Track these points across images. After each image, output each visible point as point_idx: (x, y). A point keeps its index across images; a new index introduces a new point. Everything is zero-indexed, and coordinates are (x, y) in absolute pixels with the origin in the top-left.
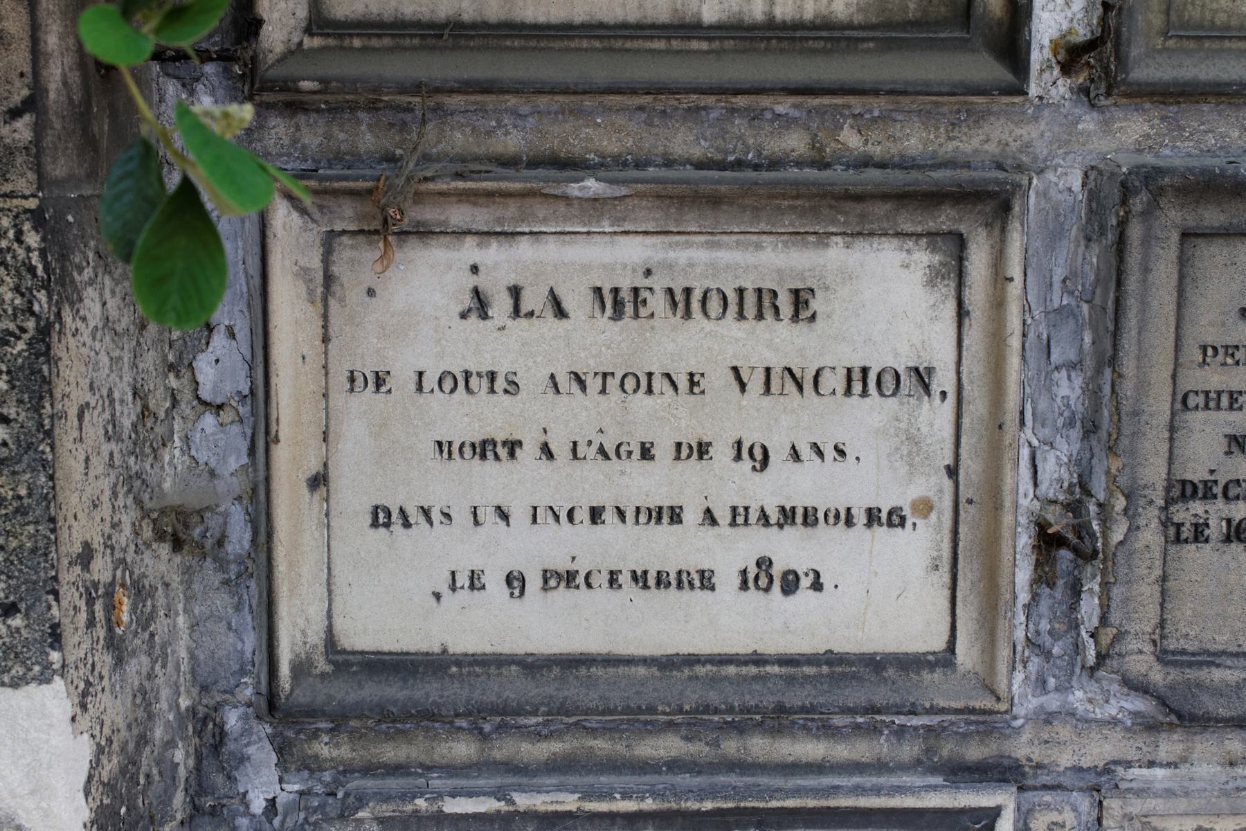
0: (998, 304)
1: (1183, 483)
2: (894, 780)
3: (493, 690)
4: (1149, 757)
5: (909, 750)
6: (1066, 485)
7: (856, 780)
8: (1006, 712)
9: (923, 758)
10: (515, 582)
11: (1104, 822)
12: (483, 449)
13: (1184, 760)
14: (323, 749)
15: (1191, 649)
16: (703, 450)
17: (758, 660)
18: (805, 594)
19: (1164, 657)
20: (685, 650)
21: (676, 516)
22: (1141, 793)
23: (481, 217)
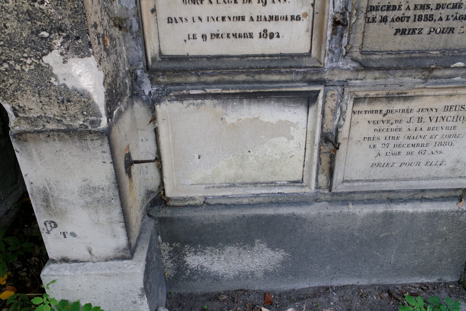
1: (371, 6)
2: (296, 85)
3: (201, 64)
4: (356, 78)
5: (299, 77)
6: (341, 8)
7: (287, 85)
8: (323, 67)
9: (303, 79)
10: (204, 37)
11: (344, 93)
13: (364, 78)
14: (161, 79)
15: (368, 50)
17: (263, 56)
18: (275, 39)
19: (362, 53)
20: (246, 53)
21: (243, 19)
22: (353, 86)
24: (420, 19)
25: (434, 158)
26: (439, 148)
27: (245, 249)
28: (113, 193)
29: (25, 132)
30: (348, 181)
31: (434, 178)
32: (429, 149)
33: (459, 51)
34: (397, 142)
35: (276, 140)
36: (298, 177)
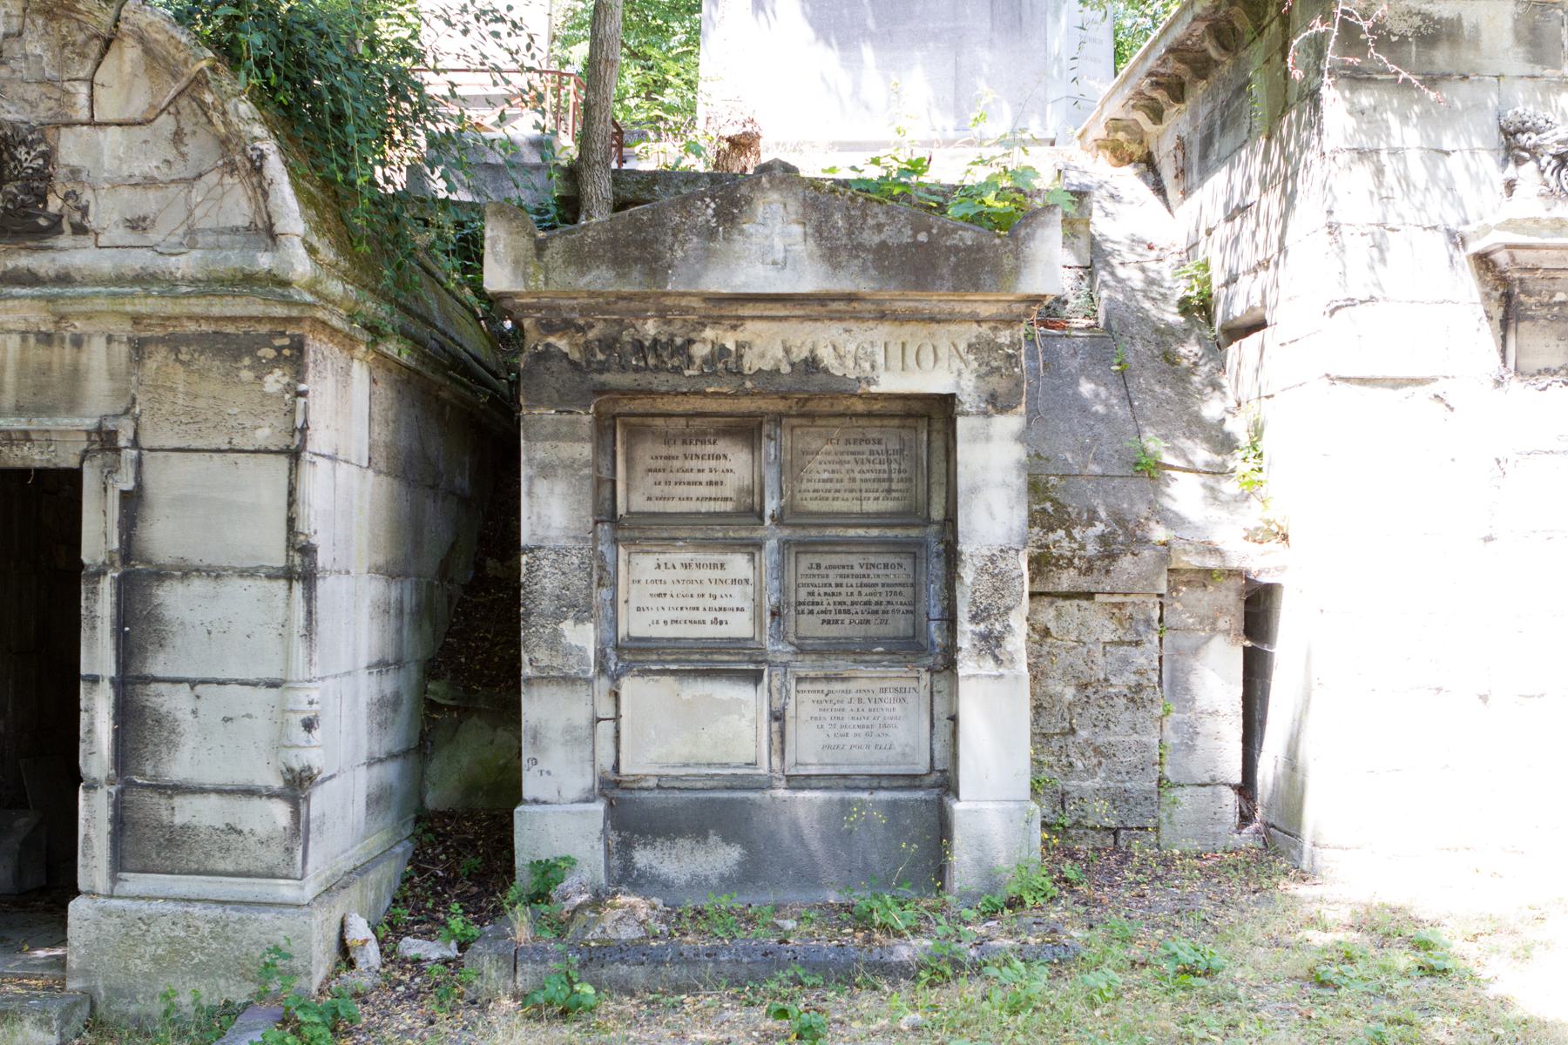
5: (746, 658)
10: (665, 622)
12: (659, 595)
19: (797, 638)
23: (659, 549)
24: (840, 612)
25: (882, 741)
26: (885, 731)
28: (589, 731)
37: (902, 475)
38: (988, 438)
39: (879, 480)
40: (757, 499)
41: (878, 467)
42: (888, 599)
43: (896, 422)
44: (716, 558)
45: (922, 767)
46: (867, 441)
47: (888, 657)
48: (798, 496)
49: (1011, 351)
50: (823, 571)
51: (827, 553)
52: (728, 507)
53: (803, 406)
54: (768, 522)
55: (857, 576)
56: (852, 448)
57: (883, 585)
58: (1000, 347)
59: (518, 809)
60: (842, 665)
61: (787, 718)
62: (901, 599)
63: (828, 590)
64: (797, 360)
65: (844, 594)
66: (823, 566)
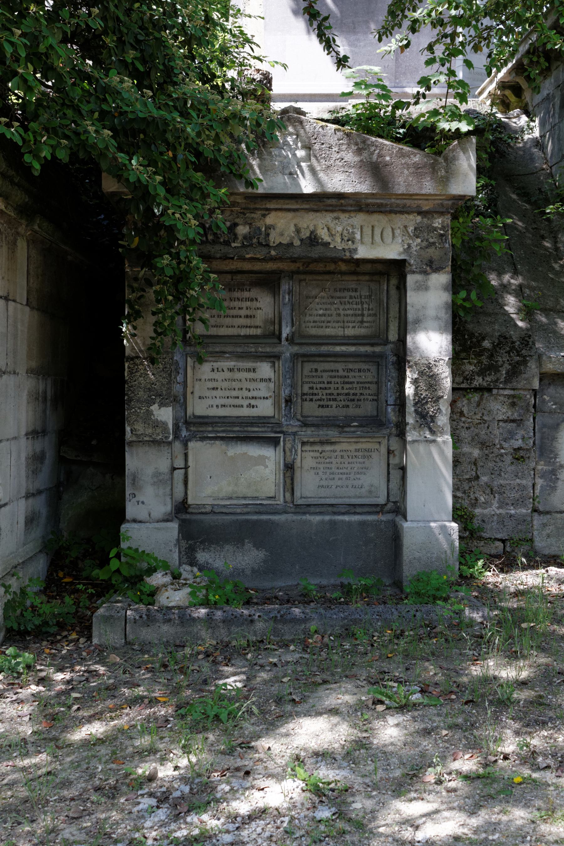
0: (279, 370)
5: (269, 429)
10: (217, 406)
12: (213, 389)
14: (192, 429)
16: (242, 389)
18: (255, 408)
19: (302, 416)
21: (238, 398)
24: (330, 400)
25: (356, 483)
26: (358, 476)
27: (238, 547)
29: (133, 441)
30: (304, 498)
31: (359, 497)
32: (352, 476)
33: (355, 417)
34: (331, 471)
35: (257, 467)
36: (272, 494)
37: (370, 312)
38: (427, 289)
39: (355, 315)
40: (277, 327)
41: (355, 306)
42: (361, 391)
43: (367, 278)
44: (250, 365)
45: (382, 500)
46: (348, 290)
47: (361, 429)
48: (304, 325)
49: (442, 232)
50: (319, 373)
51: (321, 362)
52: (259, 332)
53: (307, 267)
54: (284, 342)
55: (341, 377)
56: (338, 294)
57: (358, 383)
58: (435, 229)
59: (123, 526)
60: (332, 433)
61: (295, 468)
62: (368, 392)
63: (322, 386)
64: (304, 237)
65: (332, 388)
66: (319, 370)
